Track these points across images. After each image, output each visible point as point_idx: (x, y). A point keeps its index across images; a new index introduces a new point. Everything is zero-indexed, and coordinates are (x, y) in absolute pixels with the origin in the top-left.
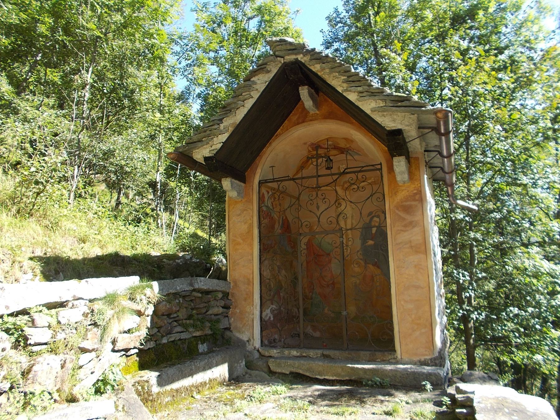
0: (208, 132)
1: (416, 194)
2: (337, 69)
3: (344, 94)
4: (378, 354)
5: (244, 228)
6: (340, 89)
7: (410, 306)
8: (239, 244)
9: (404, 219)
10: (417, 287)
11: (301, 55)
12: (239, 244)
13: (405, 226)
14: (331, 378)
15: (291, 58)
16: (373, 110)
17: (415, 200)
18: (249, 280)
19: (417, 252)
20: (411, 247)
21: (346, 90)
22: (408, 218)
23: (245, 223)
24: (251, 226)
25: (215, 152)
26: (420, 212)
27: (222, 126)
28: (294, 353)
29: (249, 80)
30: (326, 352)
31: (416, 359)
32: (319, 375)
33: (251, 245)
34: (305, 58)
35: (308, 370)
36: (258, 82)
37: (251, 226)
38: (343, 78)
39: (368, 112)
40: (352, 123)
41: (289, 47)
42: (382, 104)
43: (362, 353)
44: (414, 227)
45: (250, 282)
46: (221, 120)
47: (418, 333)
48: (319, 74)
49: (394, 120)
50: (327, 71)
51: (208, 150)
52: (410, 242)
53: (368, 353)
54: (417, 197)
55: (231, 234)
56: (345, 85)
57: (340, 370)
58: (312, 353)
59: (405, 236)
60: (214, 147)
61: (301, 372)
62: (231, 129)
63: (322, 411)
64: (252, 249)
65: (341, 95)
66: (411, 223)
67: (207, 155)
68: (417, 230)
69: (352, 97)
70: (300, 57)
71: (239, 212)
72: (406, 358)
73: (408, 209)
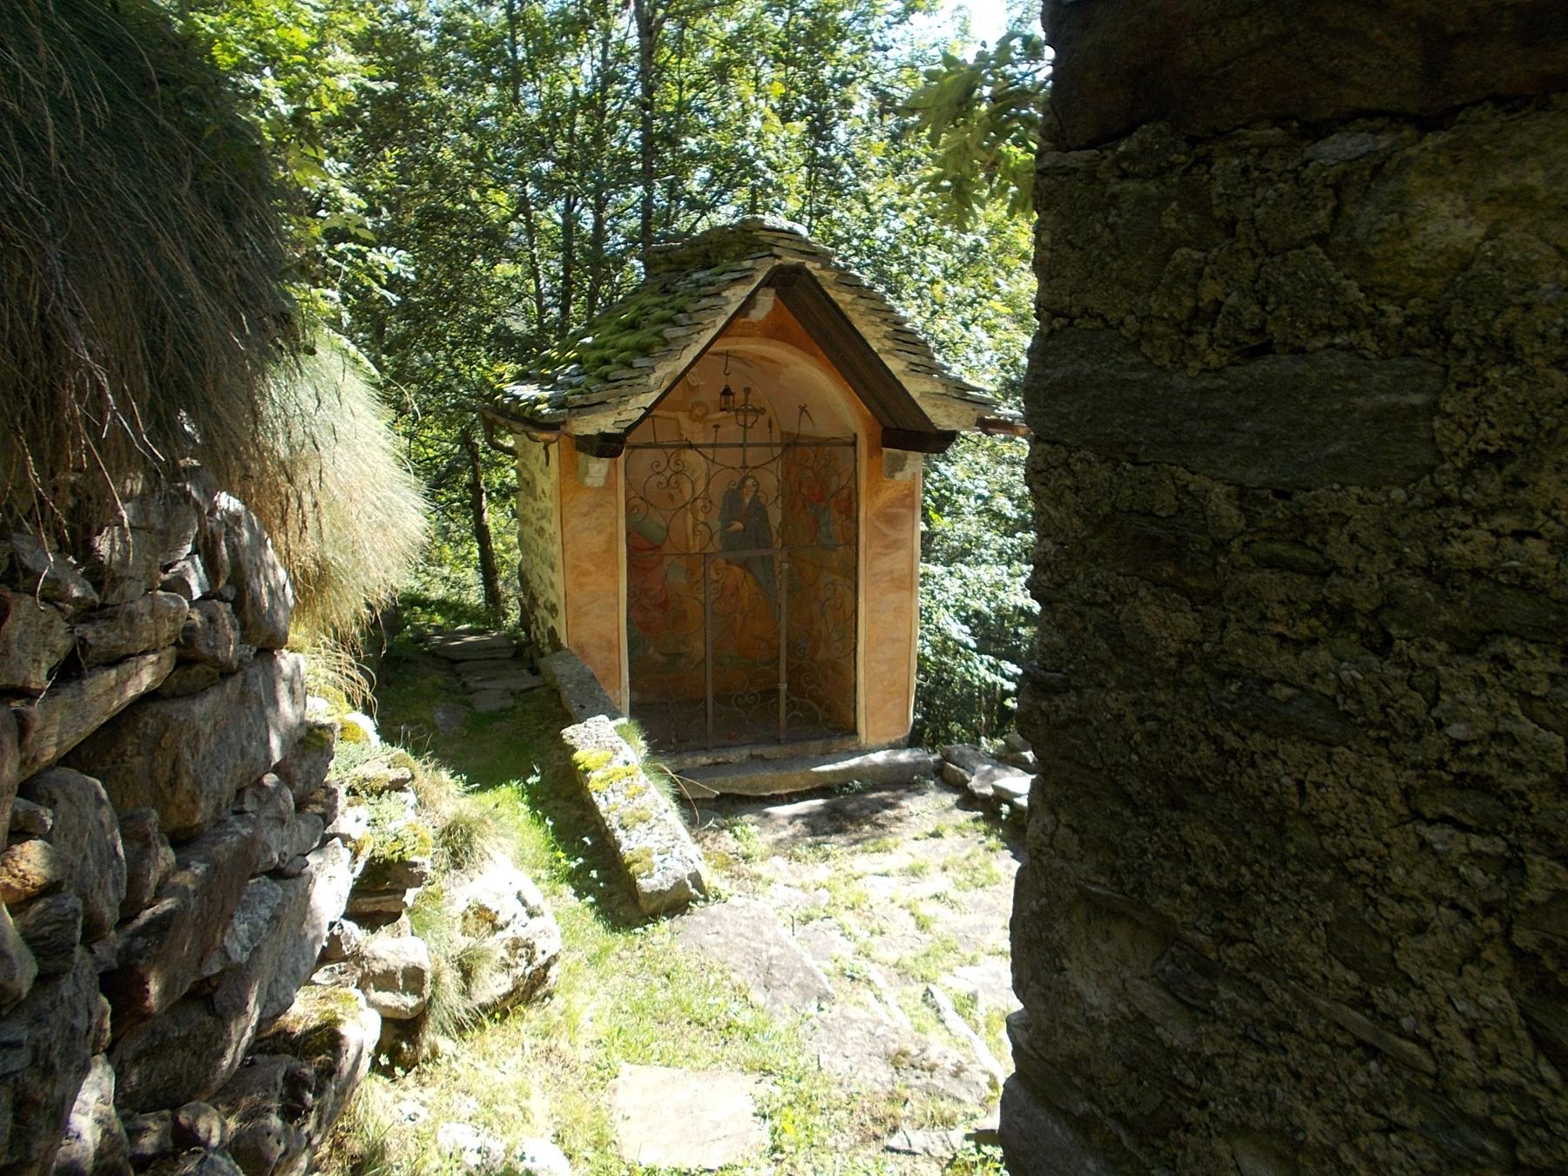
0: (626, 390)
1: (907, 496)
2: (884, 315)
3: (881, 356)
4: (836, 742)
5: (598, 541)
6: (875, 346)
7: (883, 668)
8: (586, 573)
9: (886, 535)
10: (896, 640)
11: (818, 265)
12: (586, 573)
13: (887, 547)
14: (784, 792)
15: (790, 260)
16: (922, 394)
17: (904, 506)
18: (609, 642)
19: (898, 587)
20: (892, 580)
21: (888, 352)
22: (892, 534)
23: (600, 532)
24: (613, 537)
25: (626, 425)
26: (909, 526)
27: (653, 377)
28: (703, 760)
29: (718, 294)
30: (756, 752)
31: (885, 741)
32: (766, 790)
33: (614, 576)
34: (824, 273)
35: (752, 786)
36: (733, 299)
37: (613, 537)
38: (885, 328)
39: (915, 395)
40: (815, 355)
41: (803, 248)
42: (941, 390)
43: (812, 744)
44: (899, 549)
45: (612, 646)
46: (653, 369)
47: (889, 706)
48: (841, 306)
49: (949, 416)
50: (862, 309)
51: (612, 420)
52: (892, 572)
53: (820, 743)
54: (908, 501)
55: (568, 553)
56: (889, 344)
57: (798, 779)
58: (734, 756)
59: (885, 563)
60: (622, 418)
61: (736, 791)
62: (666, 384)
63: (854, 853)
64: (617, 583)
65: (875, 355)
66: (895, 542)
67: (610, 430)
68: (902, 553)
69: (895, 365)
70: (809, 265)
71: (584, 509)
72: (872, 742)
73: (892, 520)
